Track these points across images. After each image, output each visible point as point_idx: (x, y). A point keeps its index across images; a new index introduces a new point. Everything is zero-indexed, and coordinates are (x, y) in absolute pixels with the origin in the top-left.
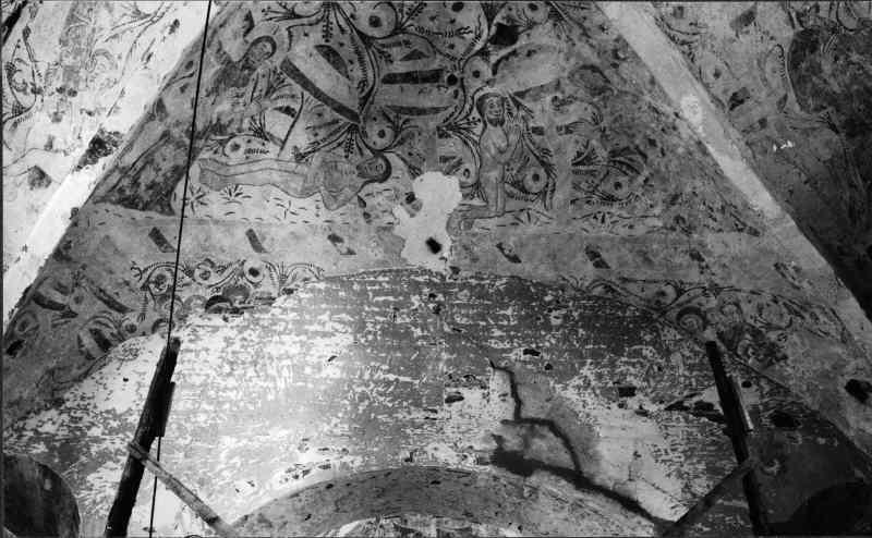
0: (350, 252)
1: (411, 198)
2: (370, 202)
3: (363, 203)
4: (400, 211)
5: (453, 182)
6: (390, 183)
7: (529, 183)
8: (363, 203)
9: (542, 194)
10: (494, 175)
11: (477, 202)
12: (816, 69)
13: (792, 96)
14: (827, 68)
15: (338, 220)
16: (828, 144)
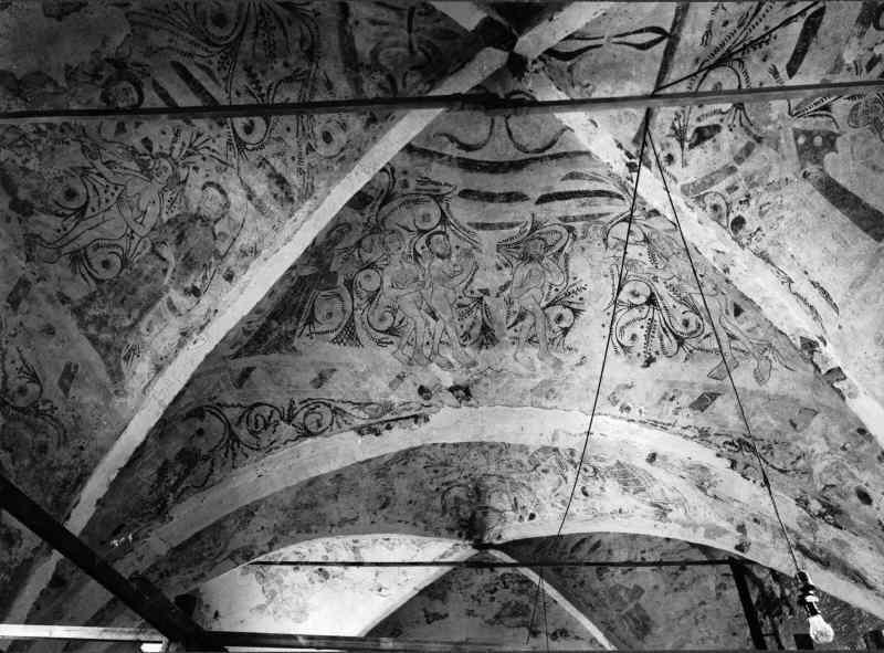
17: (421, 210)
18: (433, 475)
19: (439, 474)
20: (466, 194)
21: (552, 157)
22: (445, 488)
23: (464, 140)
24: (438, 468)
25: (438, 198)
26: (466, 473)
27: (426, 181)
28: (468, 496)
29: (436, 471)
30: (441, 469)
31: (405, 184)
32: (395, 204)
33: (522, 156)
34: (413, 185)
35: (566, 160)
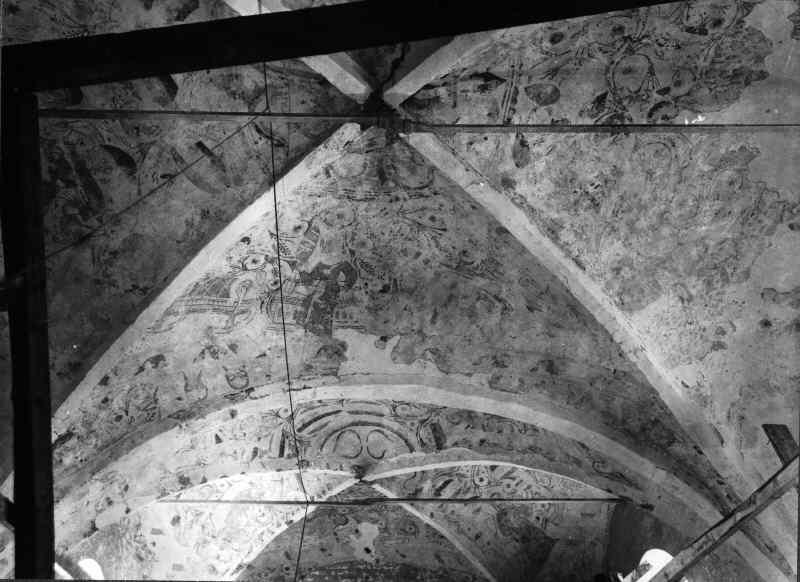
0: (330, 555)
1: (357, 531)
2: (339, 533)
3: (335, 534)
4: (352, 536)
5: (376, 527)
6: (348, 525)
7: (407, 530)
8: (335, 534)
9: (414, 533)
10: (392, 526)
11: (386, 535)
12: (507, 521)
13: (499, 532)
14: (512, 519)
15: (325, 542)
16: (515, 547)
17: (406, 413)
18: (437, 216)
19: (429, 214)
20: (382, 415)
21: (337, 431)
22: (426, 191)
23: (380, 435)
24: (431, 223)
25: (396, 416)
26: (396, 206)
27: (402, 423)
28: (395, 168)
29: (433, 219)
30: (425, 221)
31: (412, 424)
32: (420, 418)
33: (353, 428)
34: (408, 423)
35: (330, 432)
